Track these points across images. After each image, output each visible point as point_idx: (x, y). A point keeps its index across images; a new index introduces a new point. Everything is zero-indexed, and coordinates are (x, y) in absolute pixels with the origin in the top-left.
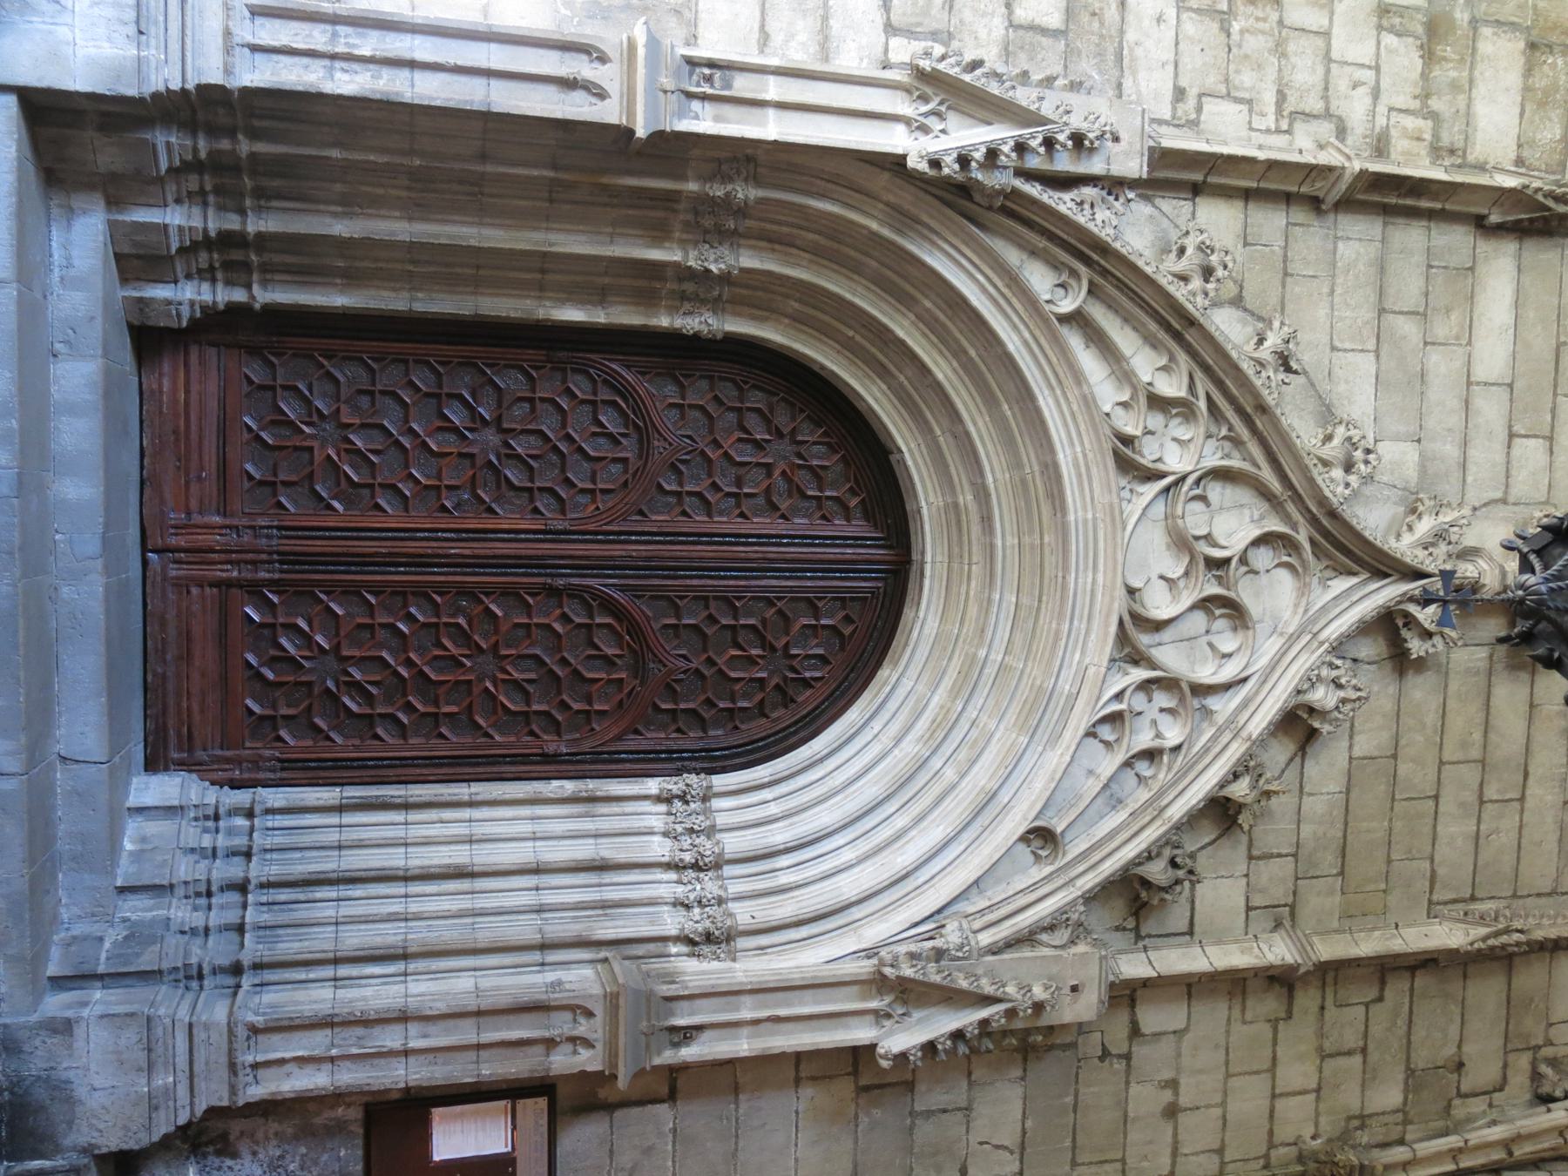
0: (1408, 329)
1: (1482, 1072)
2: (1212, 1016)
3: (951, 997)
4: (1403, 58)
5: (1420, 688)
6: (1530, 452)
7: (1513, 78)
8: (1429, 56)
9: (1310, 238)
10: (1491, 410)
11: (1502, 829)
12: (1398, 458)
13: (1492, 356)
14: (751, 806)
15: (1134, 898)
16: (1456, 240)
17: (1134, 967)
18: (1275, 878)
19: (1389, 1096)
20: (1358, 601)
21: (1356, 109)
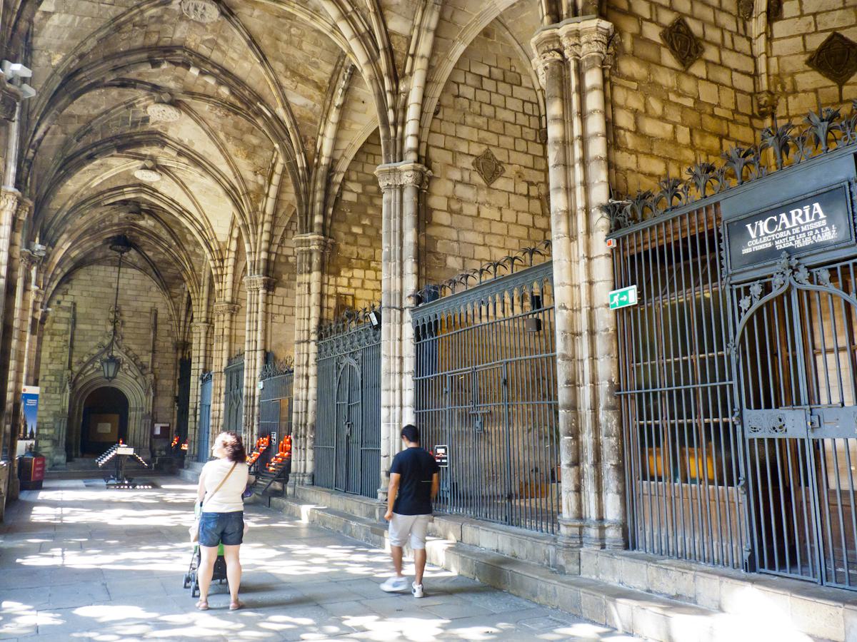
0: (86, 337)
1: (169, 327)
2: (158, 359)
3: (149, 390)
4: (56, 338)
5: (126, 336)
6: (100, 322)
7: (58, 325)
8: (56, 335)
9: (76, 349)
10: (95, 327)
11: (143, 325)
12: (100, 339)
13: (89, 327)
14: (132, 404)
15: (142, 368)
16: (76, 332)
17: (150, 369)
18: (144, 352)
19: (170, 339)
20: (115, 347)
21: (62, 344)
